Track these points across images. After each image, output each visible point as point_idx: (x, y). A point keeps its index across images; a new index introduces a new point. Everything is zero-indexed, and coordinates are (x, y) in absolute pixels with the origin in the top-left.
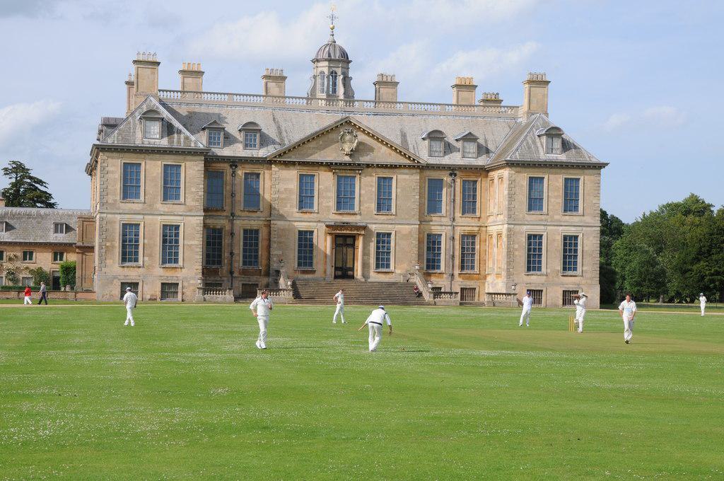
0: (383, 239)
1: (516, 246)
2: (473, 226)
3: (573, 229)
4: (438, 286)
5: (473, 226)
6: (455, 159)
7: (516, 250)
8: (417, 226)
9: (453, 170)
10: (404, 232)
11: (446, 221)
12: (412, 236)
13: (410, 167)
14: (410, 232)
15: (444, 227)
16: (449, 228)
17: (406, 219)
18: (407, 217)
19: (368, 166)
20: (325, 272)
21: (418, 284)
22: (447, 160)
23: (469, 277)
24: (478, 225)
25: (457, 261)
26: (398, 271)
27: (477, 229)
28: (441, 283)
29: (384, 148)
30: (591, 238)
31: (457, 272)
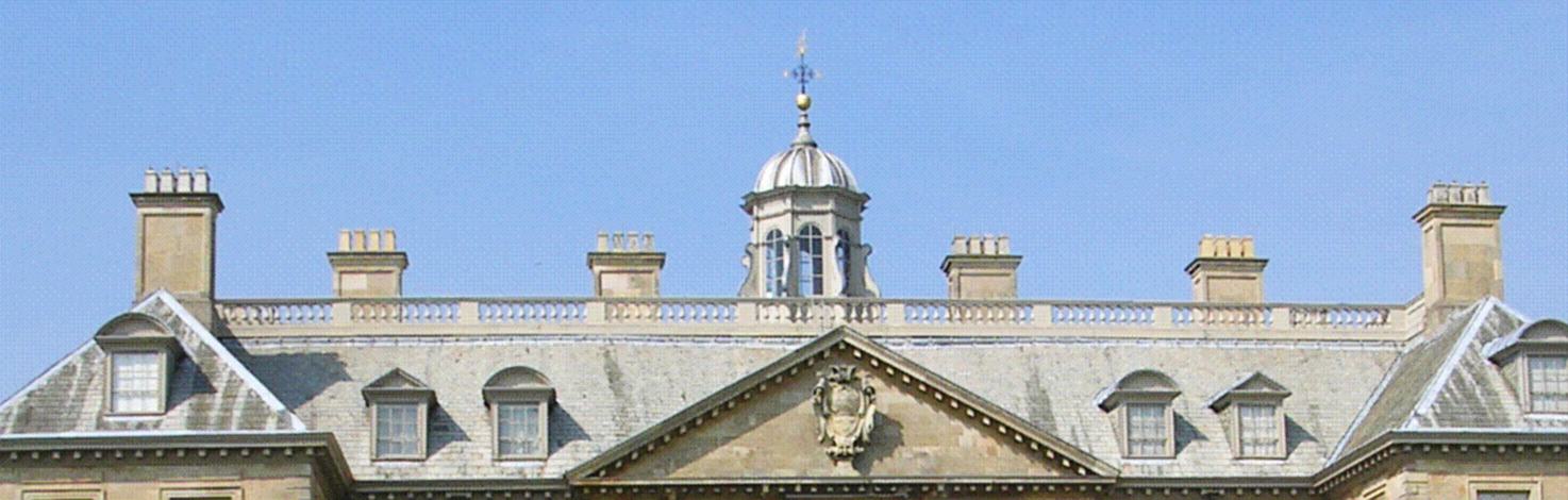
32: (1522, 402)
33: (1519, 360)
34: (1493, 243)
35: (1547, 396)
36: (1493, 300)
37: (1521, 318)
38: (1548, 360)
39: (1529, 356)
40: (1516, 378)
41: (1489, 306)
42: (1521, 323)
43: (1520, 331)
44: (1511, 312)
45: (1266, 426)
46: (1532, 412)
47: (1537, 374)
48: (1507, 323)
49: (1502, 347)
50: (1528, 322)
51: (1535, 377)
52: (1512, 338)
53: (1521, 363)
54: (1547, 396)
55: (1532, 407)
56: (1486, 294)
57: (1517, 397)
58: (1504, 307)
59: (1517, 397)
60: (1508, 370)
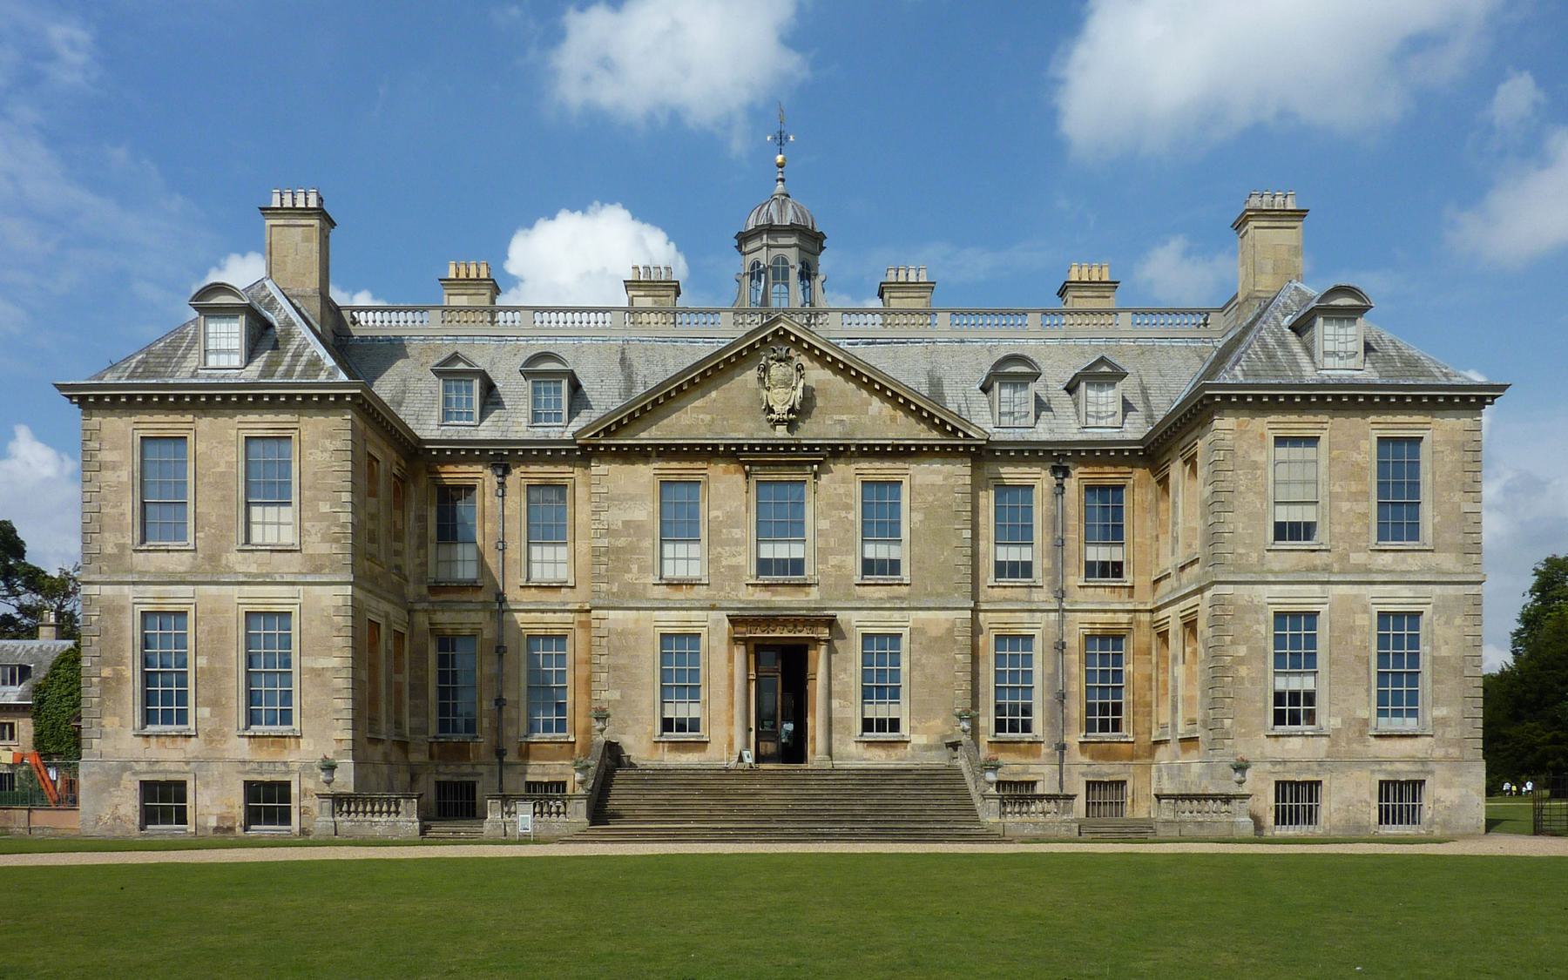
0: (881, 646)
2: (1115, 611)
4: (1026, 778)
5: (1115, 611)
6: (1063, 426)
8: (968, 614)
9: (1059, 458)
10: (934, 632)
11: (1042, 597)
12: (955, 641)
14: (950, 631)
15: (1038, 615)
16: (1053, 616)
17: (939, 595)
18: (941, 589)
19: (839, 451)
21: (964, 770)
22: (1042, 432)
23: (1105, 753)
24: (1130, 607)
25: (1076, 710)
26: (919, 739)
27: (1124, 618)
28: (1032, 769)
30: (1458, 621)
31: (1075, 737)
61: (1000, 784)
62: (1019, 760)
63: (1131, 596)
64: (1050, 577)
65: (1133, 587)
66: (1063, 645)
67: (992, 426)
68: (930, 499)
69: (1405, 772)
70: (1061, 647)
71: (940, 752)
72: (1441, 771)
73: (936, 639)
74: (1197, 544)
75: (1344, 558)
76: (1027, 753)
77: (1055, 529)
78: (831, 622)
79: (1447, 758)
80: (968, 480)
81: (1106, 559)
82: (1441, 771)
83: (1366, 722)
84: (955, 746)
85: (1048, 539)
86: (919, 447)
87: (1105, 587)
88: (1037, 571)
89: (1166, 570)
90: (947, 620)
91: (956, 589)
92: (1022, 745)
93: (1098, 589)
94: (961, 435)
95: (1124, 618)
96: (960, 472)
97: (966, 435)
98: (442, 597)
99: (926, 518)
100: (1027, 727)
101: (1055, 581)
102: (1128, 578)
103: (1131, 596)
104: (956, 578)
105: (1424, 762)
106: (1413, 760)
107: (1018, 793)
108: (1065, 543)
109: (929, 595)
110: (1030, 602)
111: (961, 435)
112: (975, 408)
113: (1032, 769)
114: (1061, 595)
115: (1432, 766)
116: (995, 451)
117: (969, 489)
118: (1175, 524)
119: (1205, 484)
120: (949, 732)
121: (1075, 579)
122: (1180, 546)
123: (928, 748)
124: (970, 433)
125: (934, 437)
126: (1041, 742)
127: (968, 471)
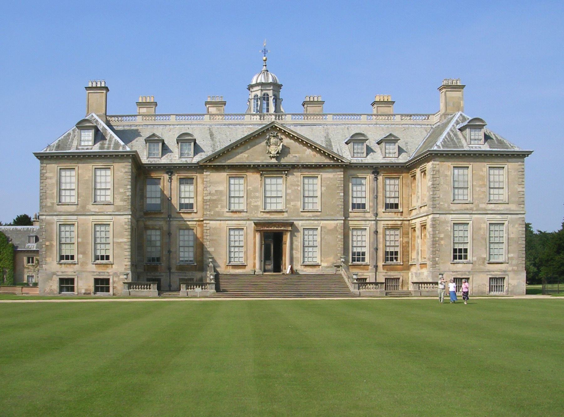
1: (442, 236)
2: (396, 220)
3: (498, 216)
5: (396, 220)
6: (377, 158)
7: (442, 239)
8: (342, 222)
10: (329, 228)
11: (370, 216)
12: (337, 231)
13: (334, 167)
14: (336, 227)
15: (368, 222)
16: (373, 222)
18: (332, 213)
19: (294, 167)
20: (254, 266)
21: (343, 275)
22: (369, 159)
24: (401, 219)
26: (324, 264)
27: (399, 223)
28: (365, 274)
29: (309, 151)
30: (517, 226)
31: (381, 264)
32: (467, 141)
33: (467, 129)
34: (461, 96)
35: (475, 140)
36: (460, 112)
37: (468, 117)
38: (476, 130)
39: (470, 128)
40: (466, 135)
41: (459, 114)
42: (468, 119)
43: (468, 121)
44: (465, 116)
45: (392, 148)
46: (470, 144)
47: (473, 133)
48: (464, 119)
49: (462, 126)
50: (470, 118)
51: (472, 134)
52: (466, 123)
53: (468, 130)
54: (475, 140)
55: (470, 143)
56: (458, 111)
57: (466, 140)
58: (463, 114)
59: (466, 140)
60: (464, 132)
61: (357, 279)
62: (361, 271)
63: (401, 215)
64: (372, 209)
65: (402, 212)
66: (377, 232)
67: (350, 157)
68: (328, 182)
69: (498, 274)
70: (376, 232)
71: (332, 269)
72: (511, 275)
73: (330, 230)
74: (426, 200)
75: (478, 205)
76: (363, 269)
77: (374, 193)
78: (292, 224)
79: (513, 270)
80: (342, 176)
81: (393, 202)
82: (511, 275)
83: (485, 259)
84: (338, 267)
85: (371, 196)
86: (324, 165)
87: (392, 212)
88: (367, 207)
89: (415, 207)
90: (334, 223)
91: (338, 213)
92: (362, 266)
93: (390, 213)
94: (340, 161)
95: (399, 223)
96: (340, 175)
97: (342, 161)
98: (149, 216)
99: (327, 189)
100: (363, 260)
101: (374, 210)
102: (400, 209)
103: (401, 215)
104: (338, 209)
105: (505, 271)
106: (501, 271)
107: (362, 282)
108: (378, 197)
109: (328, 215)
110: (365, 217)
111: (340, 161)
112: (343, 150)
113: (365, 274)
114: (377, 215)
115: (507, 273)
116: (352, 166)
117: (343, 179)
118: (418, 192)
119: (429, 181)
120: (335, 262)
121: (381, 209)
122: (420, 200)
123: (327, 267)
124: (343, 160)
125: (327, 161)
126: (369, 265)
127: (342, 173)
